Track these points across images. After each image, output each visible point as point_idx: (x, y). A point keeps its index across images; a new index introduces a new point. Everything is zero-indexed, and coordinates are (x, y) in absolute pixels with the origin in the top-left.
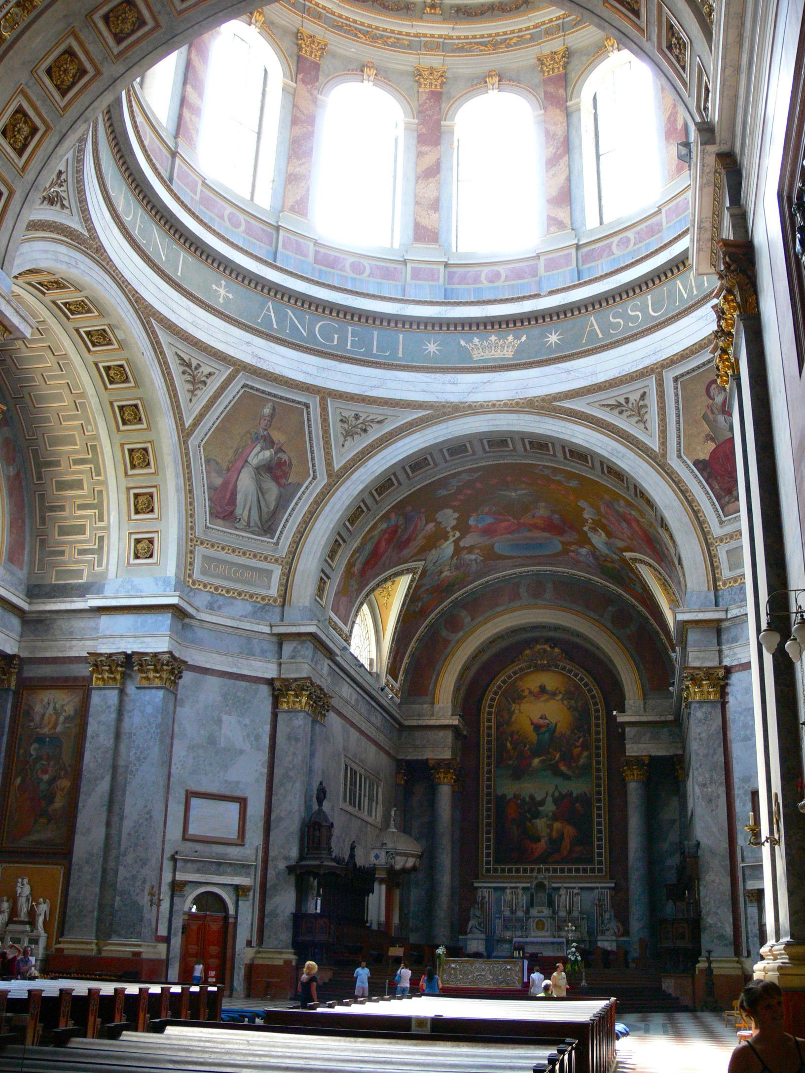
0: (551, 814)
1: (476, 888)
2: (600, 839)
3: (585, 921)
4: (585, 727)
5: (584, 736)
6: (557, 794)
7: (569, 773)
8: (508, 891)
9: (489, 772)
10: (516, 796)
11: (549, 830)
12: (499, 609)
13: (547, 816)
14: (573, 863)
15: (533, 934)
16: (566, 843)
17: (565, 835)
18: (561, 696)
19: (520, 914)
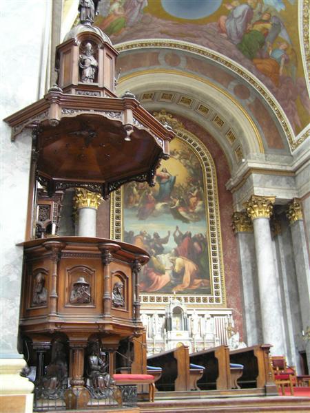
0: (173, 250)
2: (216, 273)
4: (199, 182)
5: (199, 188)
6: (177, 234)
7: (187, 217)
9: (118, 211)
10: (142, 234)
11: (172, 264)
12: (141, 69)
13: (170, 252)
14: (193, 293)
16: (187, 277)
17: (186, 269)
18: (178, 156)
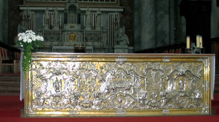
1: (22, 11)
3: (105, 34)
8: (47, 12)
15: (67, 44)
19: (56, 29)
